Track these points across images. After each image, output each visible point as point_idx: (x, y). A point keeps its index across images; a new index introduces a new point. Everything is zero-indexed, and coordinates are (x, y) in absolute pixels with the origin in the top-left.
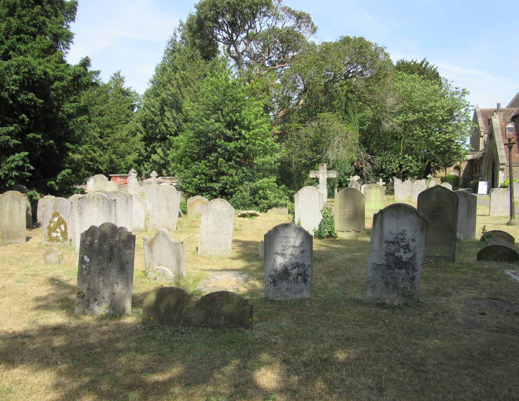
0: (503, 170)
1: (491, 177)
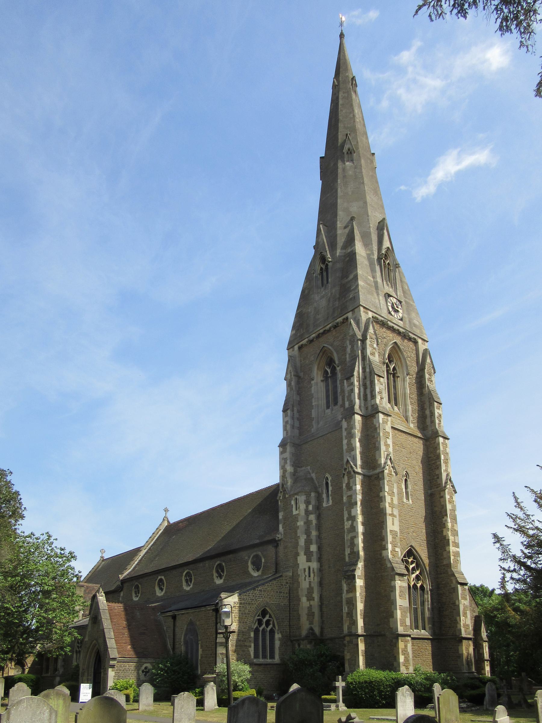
0: (113, 666)
1: (91, 677)
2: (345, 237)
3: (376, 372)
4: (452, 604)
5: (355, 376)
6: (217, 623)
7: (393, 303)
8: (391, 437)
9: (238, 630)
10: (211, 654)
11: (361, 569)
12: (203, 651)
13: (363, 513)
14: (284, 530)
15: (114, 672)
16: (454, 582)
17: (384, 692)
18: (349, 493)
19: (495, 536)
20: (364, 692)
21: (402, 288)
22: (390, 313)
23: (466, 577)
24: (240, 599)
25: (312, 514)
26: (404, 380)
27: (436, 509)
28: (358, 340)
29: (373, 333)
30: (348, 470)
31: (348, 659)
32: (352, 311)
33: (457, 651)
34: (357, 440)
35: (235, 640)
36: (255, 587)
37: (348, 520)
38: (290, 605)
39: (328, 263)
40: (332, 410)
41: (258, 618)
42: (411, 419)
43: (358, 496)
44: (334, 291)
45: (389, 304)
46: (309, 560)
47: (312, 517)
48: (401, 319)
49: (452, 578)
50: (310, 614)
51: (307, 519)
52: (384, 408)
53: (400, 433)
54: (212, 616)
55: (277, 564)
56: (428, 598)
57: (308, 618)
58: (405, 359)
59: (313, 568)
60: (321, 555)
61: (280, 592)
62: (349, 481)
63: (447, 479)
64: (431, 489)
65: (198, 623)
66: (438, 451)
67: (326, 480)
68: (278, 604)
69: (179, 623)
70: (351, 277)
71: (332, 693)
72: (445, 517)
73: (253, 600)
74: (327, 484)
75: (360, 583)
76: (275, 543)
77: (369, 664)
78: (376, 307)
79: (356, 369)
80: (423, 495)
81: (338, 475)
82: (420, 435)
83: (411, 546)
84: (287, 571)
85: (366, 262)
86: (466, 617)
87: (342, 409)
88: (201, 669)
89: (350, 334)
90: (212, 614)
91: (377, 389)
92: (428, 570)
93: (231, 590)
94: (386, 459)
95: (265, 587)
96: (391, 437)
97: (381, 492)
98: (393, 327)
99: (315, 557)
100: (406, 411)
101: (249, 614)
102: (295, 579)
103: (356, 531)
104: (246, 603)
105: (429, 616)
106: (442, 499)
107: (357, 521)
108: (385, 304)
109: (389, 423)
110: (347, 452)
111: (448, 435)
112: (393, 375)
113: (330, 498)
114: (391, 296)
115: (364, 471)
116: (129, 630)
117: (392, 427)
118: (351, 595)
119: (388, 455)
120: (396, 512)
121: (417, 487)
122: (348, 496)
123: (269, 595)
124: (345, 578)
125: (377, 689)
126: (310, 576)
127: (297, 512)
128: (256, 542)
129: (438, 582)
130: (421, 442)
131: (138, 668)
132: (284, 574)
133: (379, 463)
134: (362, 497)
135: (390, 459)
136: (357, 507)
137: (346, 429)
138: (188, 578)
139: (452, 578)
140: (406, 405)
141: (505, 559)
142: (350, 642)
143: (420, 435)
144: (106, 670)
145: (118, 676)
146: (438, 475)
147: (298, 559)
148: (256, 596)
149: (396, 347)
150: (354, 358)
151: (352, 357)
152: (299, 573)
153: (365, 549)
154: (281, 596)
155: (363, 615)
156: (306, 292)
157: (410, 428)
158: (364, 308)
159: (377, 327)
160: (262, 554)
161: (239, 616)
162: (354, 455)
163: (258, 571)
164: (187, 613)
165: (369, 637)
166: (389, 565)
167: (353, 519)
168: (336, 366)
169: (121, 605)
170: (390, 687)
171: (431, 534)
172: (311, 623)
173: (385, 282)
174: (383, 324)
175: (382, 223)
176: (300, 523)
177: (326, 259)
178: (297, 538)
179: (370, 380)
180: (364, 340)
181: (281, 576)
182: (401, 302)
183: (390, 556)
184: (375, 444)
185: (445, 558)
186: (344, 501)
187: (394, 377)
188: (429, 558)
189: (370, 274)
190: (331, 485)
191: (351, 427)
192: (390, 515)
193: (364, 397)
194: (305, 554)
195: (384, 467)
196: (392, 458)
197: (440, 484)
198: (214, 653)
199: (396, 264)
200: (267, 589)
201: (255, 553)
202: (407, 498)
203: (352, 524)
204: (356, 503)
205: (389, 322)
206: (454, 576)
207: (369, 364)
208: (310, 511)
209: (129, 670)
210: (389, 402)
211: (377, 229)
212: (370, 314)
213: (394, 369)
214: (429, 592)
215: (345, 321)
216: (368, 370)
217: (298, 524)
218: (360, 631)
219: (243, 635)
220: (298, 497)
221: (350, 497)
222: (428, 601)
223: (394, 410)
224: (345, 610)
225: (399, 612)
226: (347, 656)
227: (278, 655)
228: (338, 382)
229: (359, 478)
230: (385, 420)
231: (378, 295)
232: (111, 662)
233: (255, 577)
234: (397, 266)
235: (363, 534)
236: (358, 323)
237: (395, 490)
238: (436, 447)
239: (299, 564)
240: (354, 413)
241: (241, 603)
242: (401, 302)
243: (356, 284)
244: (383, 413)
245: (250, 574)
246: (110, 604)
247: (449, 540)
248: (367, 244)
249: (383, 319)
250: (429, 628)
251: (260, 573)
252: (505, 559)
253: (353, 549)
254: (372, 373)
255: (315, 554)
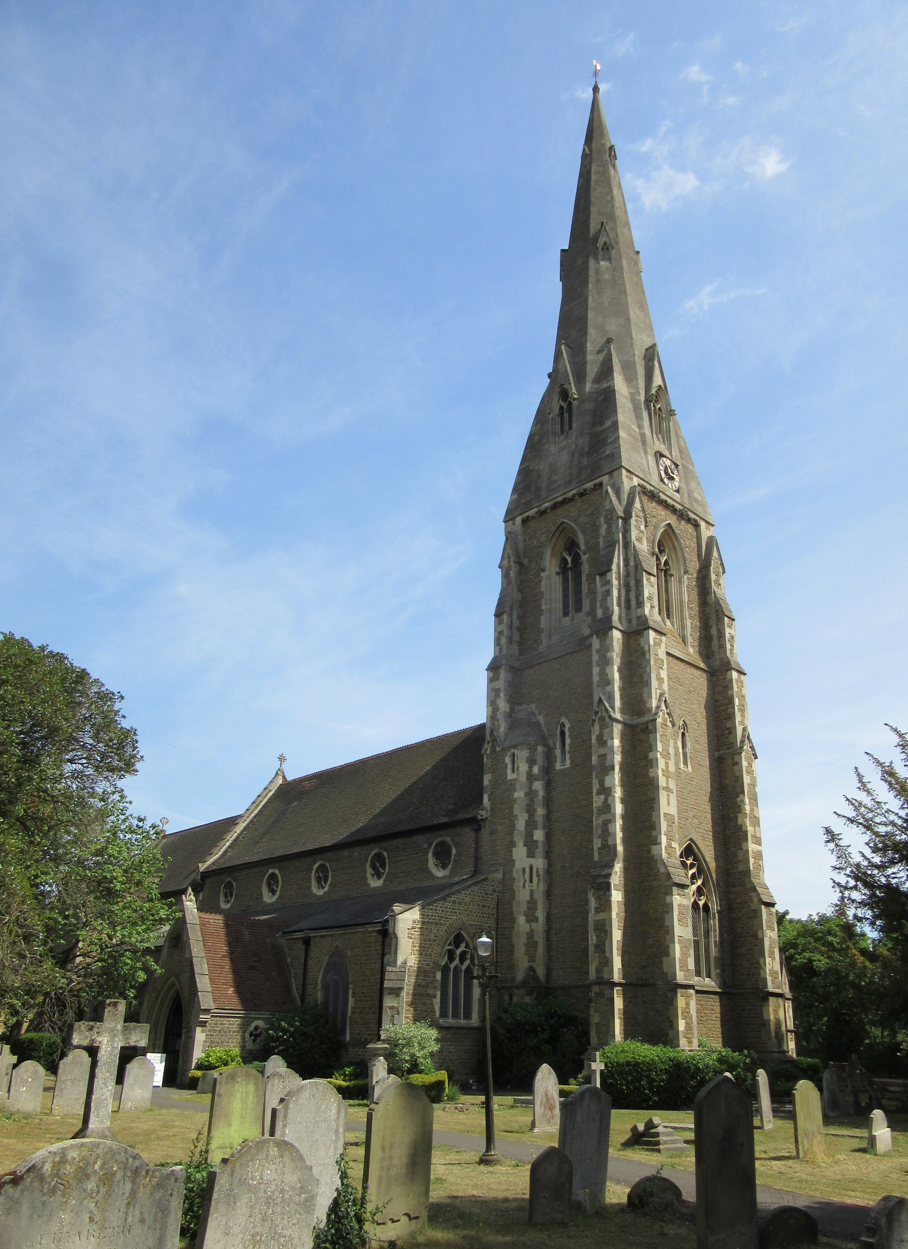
0: (203, 1024)
2: (598, 366)
3: (645, 567)
4: (752, 936)
5: (614, 571)
6: (383, 955)
7: (666, 466)
8: (665, 667)
9: (418, 967)
10: (370, 1008)
11: (618, 873)
12: (356, 1001)
13: (623, 784)
14: (492, 804)
15: (204, 1034)
16: (755, 900)
17: (657, 1081)
18: (602, 751)
19: (828, 831)
20: (626, 1080)
21: (678, 445)
22: (662, 480)
23: (773, 894)
24: (422, 915)
25: (538, 780)
26: (680, 581)
27: (727, 782)
28: (618, 517)
29: (640, 508)
30: (600, 715)
31: (597, 1024)
32: (609, 473)
33: (761, 1015)
34: (616, 668)
35: (412, 984)
36: (446, 895)
37: (599, 793)
38: (497, 928)
39: (572, 401)
40: (573, 619)
41: (449, 947)
42: (690, 640)
43: (616, 756)
44: (580, 441)
45: (662, 468)
46: (531, 854)
47: (538, 786)
48: (678, 491)
49: (752, 894)
50: (531, 945)
51: (530, 788)
52: (655, 622)
53: (676, 661)
54: (377, 942)
55: (477, 859)
56: (715, 926)
57: (526, 951)
58: (682, 550)
59: (537, 869)
60: (549, 847)
61: (484, 906)
62: (602, 732)
63: (743, 736)
64: (718, 750)
65: (349, 953)
66: (730, 692)
67: (561, 727)
68: (480, 925)
69: (314, 951)
70: (608, 423)
71: (572, 1081)
72: (741, 796)
73: (442, 917)
74: (563, 733)
75: (617, 896)
76: (476, 824)
77: (628, 1034)
78: (644, 471)
79: (615, 560)
80: (707, 759)
81: (580, 721)
82: (702, 665)
83: (691, 840)
84: (495, 871)
85: (629, 405)
86: (773, 959)
87: (589, 619)
88: (351, 1034)
89: (606, 509)
90: (375, 938)
91: (646, 594)
92: (714, 878)
93: (409, 899)
94: (659, 701)
95: (461, 896)
96: (665, 667)
97: (651, 751)
98: (666, 502)
99: (540, 850)
100: (683, 627)
101: (434, 941)
102: (507, 887)
103: (612, 812)
104: (432, 923)
105: (717, 955)
106: (736, 768)
107: (614, 797)
108: (656, 468)
109: (663, 645)
110: (598, 686)
111: (745, 668)
112: (665, 572)
113: (568, 756)
114: (664, 456)
115: (626, 717)
116: (233, 960)
117: (668, 654)
118: (601, 916)
119: (661, 695)
120: (672, 785)
121: (698, 746)
122: (599, 756)
123: (466, 910)
124: (593, 887)
125: (646, 1077)
126: (531, 881)
127: (514, 776)
128: (443, 821)
129: (728, 899)
130: (705, 676)
131: (244, 1027)
132: (490, 876)
133: (648, 706)
134: (622, 758)
135: (665, 701)
136: (614, 773)
137: (598, 651)
138: (321, 875)
139: (752, 894)
140: (682, 619)
141: (842, 868)
142: (600, 995)
143: (702, 665)
144: (191, 1031)
145: (210, 1042)
146: (730, 728)
147: (514, 852)
148: (447, 912)
149: (669, 530)
150: (611, 545)
151: (609, 541)
152: (515, 875)
153: (625, 840)
154: (485, 913)
155: (621, 949)
156: (536, 438)
157: (688, 654)
158: (628, 470)
159: (645, 499)
160: (453, 841)
161: (421, 943)
162: (609, 692)
163: (444, 867)
164: (331, 935)
165: (628, 987)
166: (662, 870)
167: (607, 792)
168: (581, 553)
169: (220, 917)
170: (666, 1073)
171: (719, 822)
172: (532, 959)
173: (654, 436)
174: (653, 496)
175: (650, 351)
176: (519, 794)
177: (570, 394)
178: (512, 819)
179: (636, 578)
180: (627, 518)
181: (486, 879)
182: (677, 466)
183: (664, 855)
184: (641, 676)
185: (740, 862)
186: (593, 763)
187: (665, 576)
188: (716, 860)
189: (634, 421)
190: (570, 736)
191: (606, 648)
192: (664, 788)
193: (625, 603)
194: (526, 844)
195: (656, 714)
196: (667, 699)
197: (733, 743)
198: (377, 1005)
199: (671, 411)
200: (463, 899)
201: (440, 839)
202: (685, 763)
203: (606, 800)
204: (613, 768)
205: (661, 494)
206: (756, 890)
207: (634, 553)
208: (536, 775)
209: (230, 1032)
210: (660, 614)
211: (644, 358)
212: (636, 481)
213: (666, 563)
214: (717, 915)
215: (597, 487)
216: (632, 563)
217: (516, 795)
218: (617, 977)
219: (426, 976)
220: (516, 752)
221: (603, 757)
222: (715, 930)
223: (665, 625)
224: (592, 938)
225: (677, 947)
226: (595, 1018)
227: (476, 1013)
228: (584, 578)
229: (617, 729)
230: (658, 641)
231: (646, 453)
232: (201, 1016)
233: (438, 878)
234: (672, 413)
235: (623, 817)
236: (618, 493)
237: (671, 751)
238: (727, 686)
239: (514, 860)
240: (611, 628)
241: (423, 923)
242: (677, 466)
243: (616, 435)
244: (655, 630)
245: (430, 873)
246: (203, 915)
247: (746, 831)
248: (630, 379)
249: (653, 489)
250: (717, 974)
251: (447, 872)
252: (842, 868)
253: (607, 841)
254: (638, 567)
255: (540, 846)
